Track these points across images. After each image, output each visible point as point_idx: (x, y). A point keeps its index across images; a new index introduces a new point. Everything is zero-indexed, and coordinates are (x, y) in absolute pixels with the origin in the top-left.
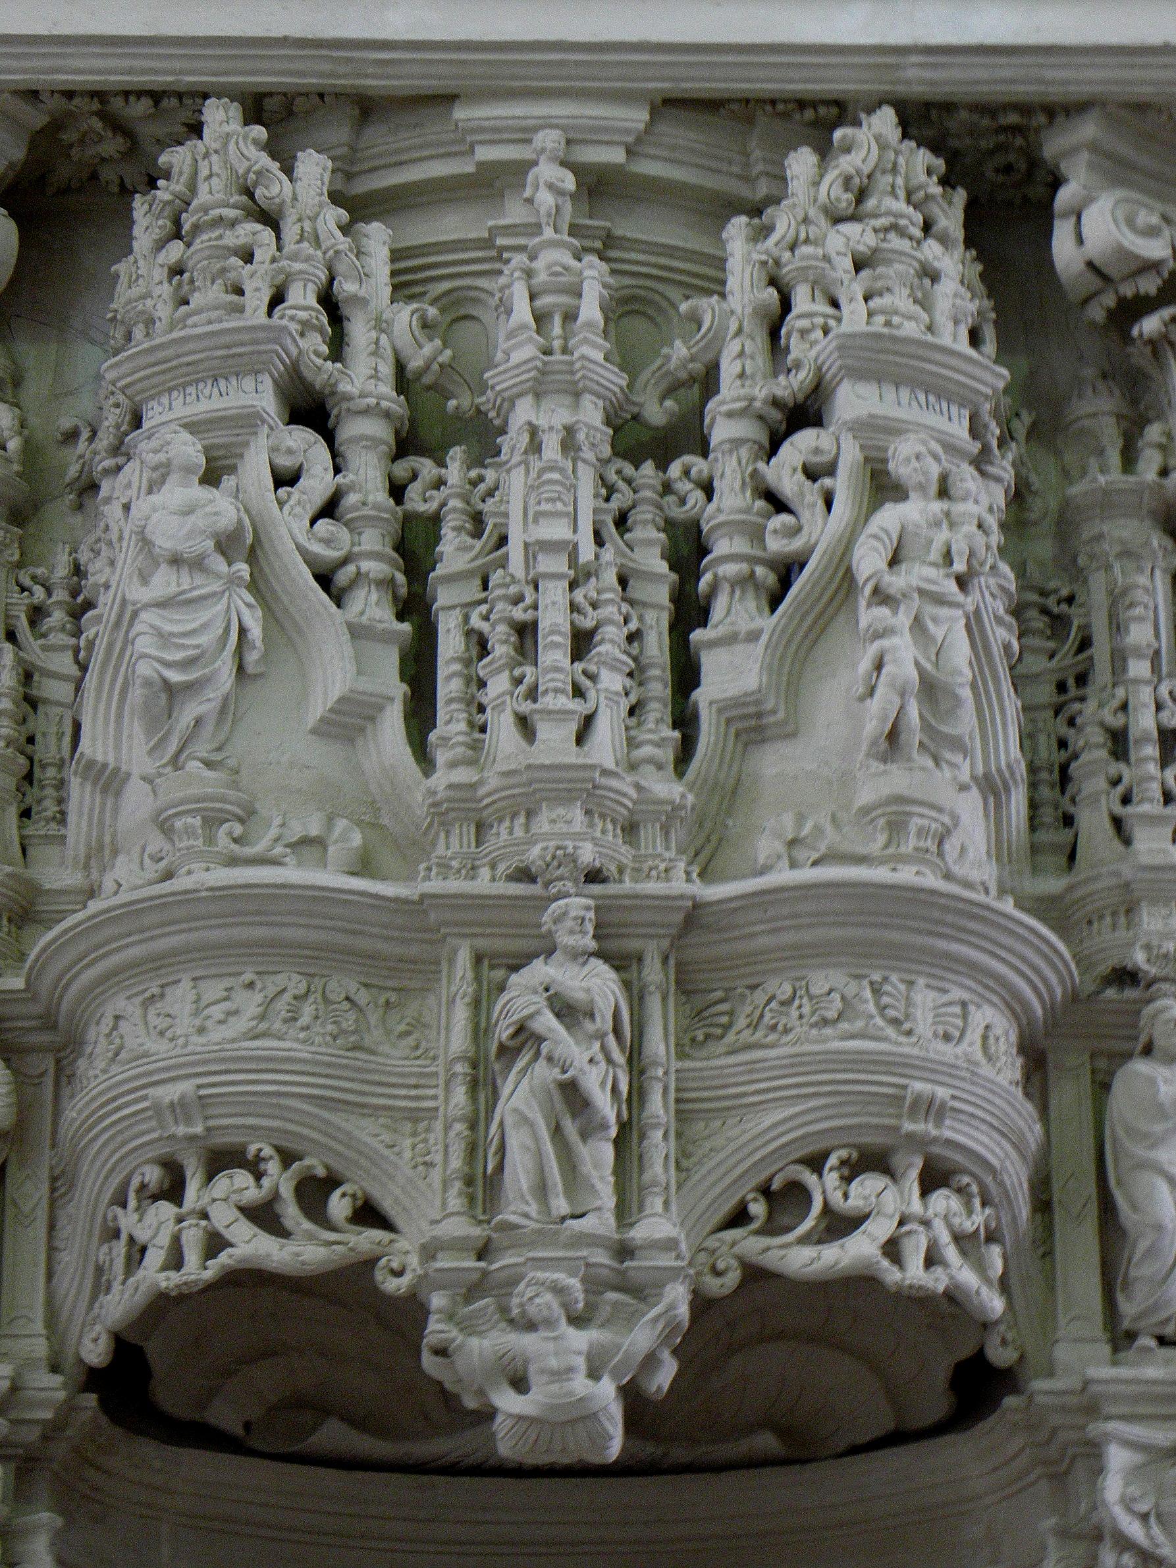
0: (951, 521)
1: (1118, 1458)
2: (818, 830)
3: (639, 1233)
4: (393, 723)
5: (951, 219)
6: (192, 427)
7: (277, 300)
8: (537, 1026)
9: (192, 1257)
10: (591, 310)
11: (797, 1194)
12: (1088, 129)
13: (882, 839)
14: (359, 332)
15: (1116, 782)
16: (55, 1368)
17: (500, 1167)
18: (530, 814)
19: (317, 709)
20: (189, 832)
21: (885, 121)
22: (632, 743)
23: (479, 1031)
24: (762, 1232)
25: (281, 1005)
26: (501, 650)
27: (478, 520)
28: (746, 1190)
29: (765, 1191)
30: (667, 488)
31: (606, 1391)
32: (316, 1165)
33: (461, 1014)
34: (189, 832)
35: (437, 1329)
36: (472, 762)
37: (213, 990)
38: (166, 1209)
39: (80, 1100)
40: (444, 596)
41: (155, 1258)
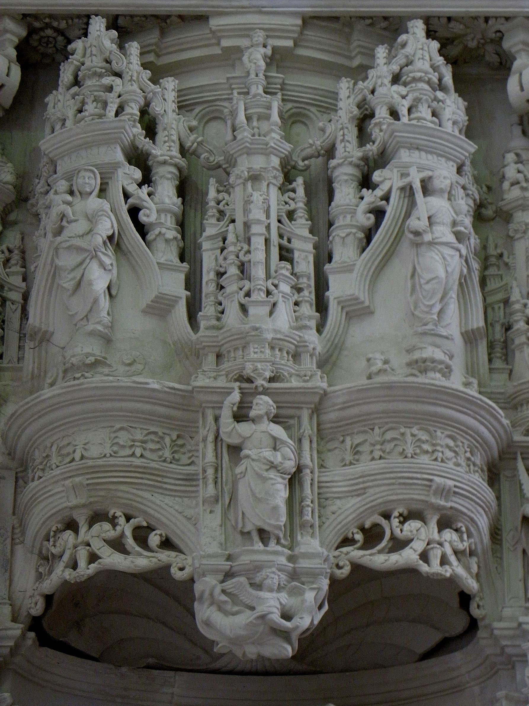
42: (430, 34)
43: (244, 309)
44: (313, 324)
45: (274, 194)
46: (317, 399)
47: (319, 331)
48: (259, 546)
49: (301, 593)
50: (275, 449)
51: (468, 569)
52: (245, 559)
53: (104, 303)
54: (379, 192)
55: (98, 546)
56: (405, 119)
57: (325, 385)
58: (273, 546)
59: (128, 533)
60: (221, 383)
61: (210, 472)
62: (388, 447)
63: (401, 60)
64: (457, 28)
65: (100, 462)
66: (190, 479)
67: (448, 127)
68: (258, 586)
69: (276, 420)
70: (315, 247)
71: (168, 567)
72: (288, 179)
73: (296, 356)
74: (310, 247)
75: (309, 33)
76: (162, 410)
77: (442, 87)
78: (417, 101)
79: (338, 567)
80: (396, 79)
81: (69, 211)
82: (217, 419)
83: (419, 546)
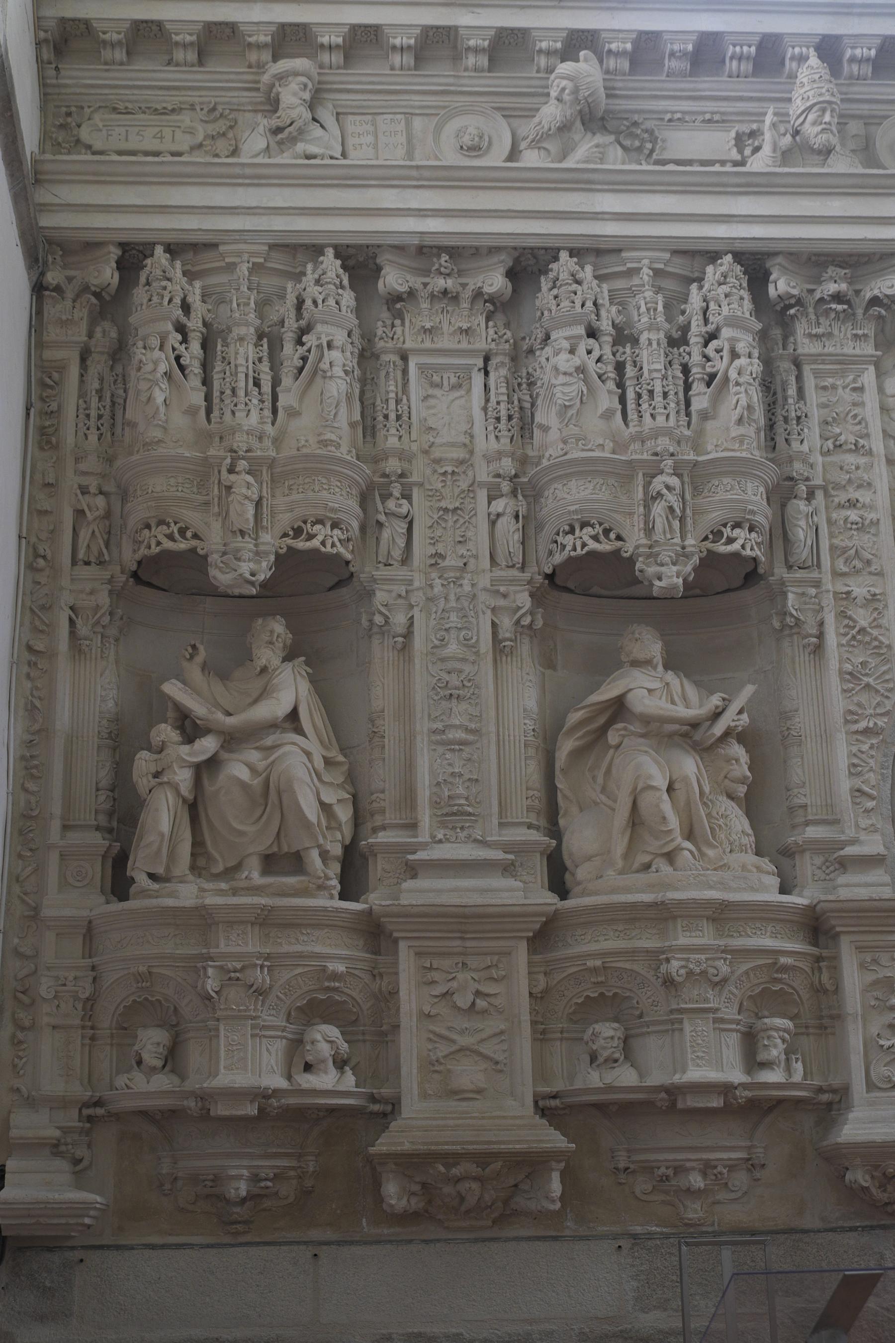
0: (751, 364)
1: (791, 596)
2: (722, 443)
3: (686, 543)
4: (619, 414)
5: (745, 285)
6: (566, 338)
7: (583, 305)
8: (662, 492)
9: (579, 548)
10: (660, 308)
11: (720, 534)
12: (780, 259)
13: (737, 445)
14: (603, 313)
15: (786, 430)
16: (539, 574)
17: (653, 527)
18: (656, 439)
19: (600, 411)
20: (572, 443)
21: (729, 258)
22: (678, 421)
23: (646, 492)
24: (713, 542)
25: (598, 486)
26: (645, 397)
27: (635, 362)
28: (708, 532)
29: (712, 532)
30: (680, 355)
31: (681, 581)
32: (606, 525)
33: (641, 489)
34: (572, 443)
35: (638, 566)
36: (639, 426)
37: (581, 483)
38: (570, 536)
39: (546, 509)
40: (628, 383)
41: (568, 548)
42: (337, 256)
43: (233, 413)
44: (269, 420)
45: (251, 348)
46: (270, 461)
47: (273, 424)
48: (240, 539)
49: (260, 563)
50: (248, 488)
51: (346, 548)
52: (233, 545)
53: (162, 409)
54: (305, 348)
55: (161, 538)
56: (320, 306)
57: (274, 454)
58: (247, 538)
59: (176, 531)
60: (222, 453)
61: (216, 499)
62: (306, 487)
63: (319, 271)
64: (351, 251)
65: (160, 495)
66: (207, 504)
67: (344, 309)
68: (239, 559)
69: (248, 473)
70: (272, 378)
71: (196, 548)
72: (260, 337)
73: (260, 438)
74: (269, 378)
75: (273, 254)
76: (191, 467)
77: (342, 287)
78: (328, 295)
79: (281, 548)
80: (318, 282)
81: (144, 359)
82: (219, 472)
83: (320, 538)
